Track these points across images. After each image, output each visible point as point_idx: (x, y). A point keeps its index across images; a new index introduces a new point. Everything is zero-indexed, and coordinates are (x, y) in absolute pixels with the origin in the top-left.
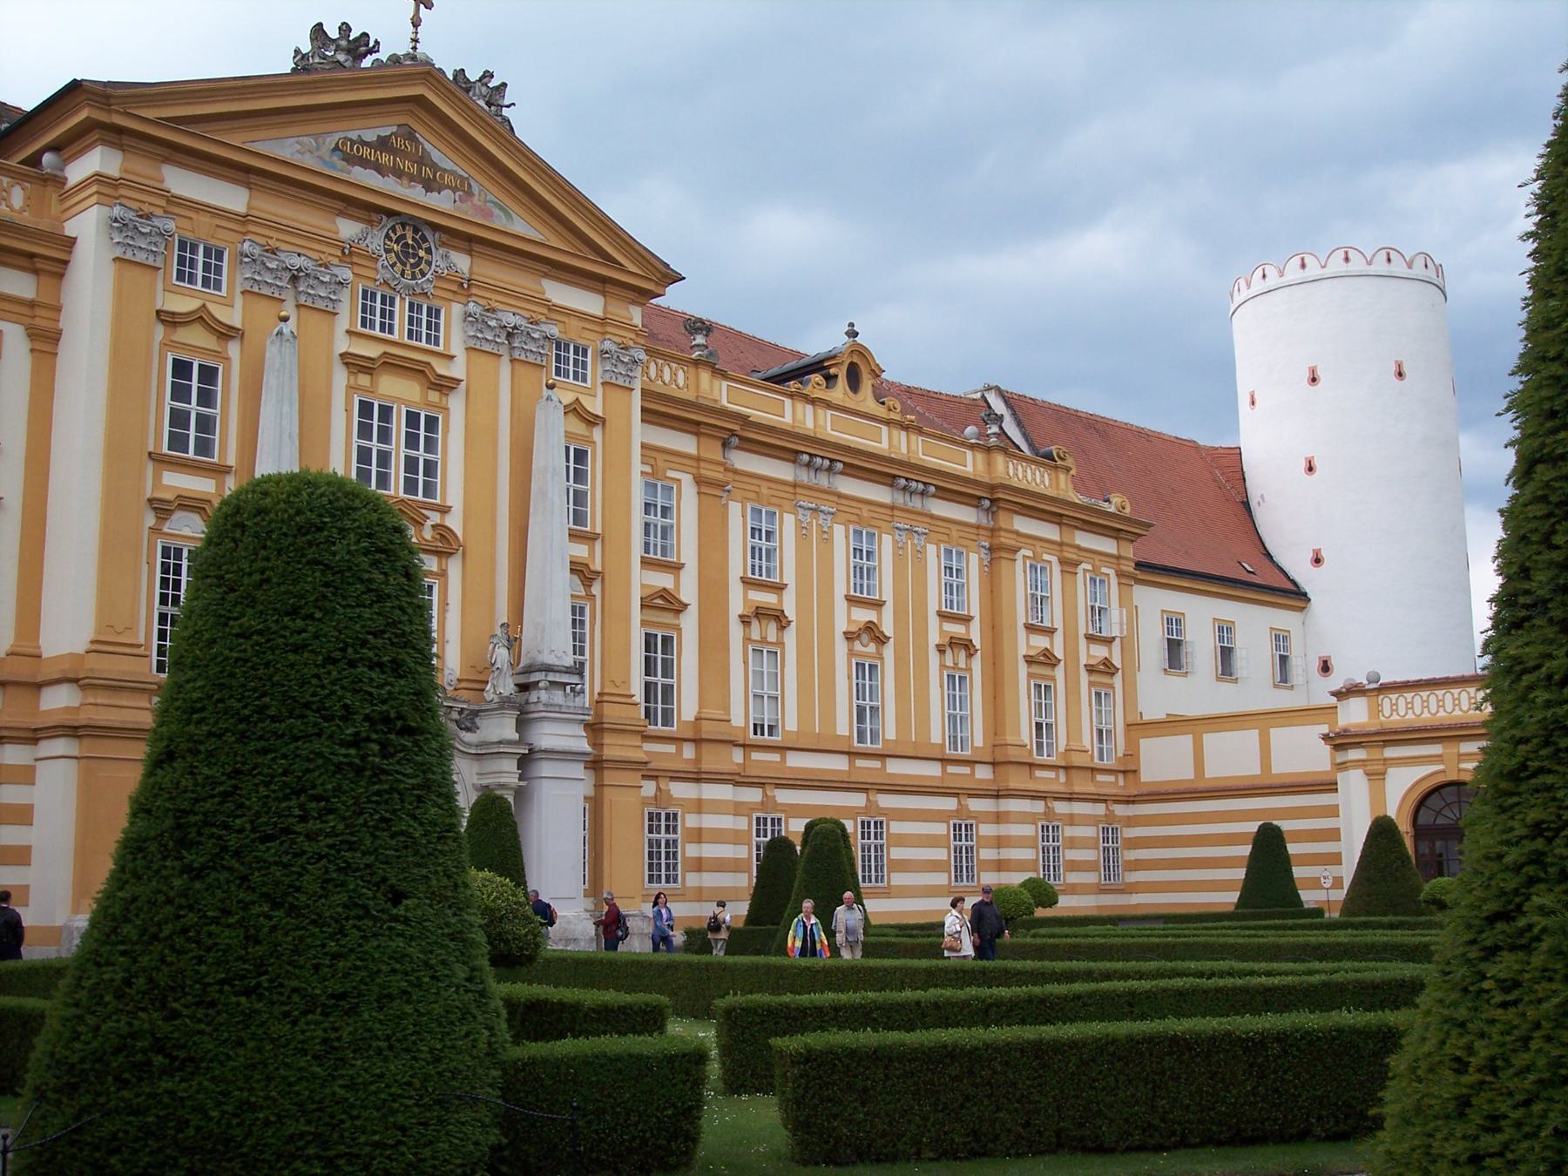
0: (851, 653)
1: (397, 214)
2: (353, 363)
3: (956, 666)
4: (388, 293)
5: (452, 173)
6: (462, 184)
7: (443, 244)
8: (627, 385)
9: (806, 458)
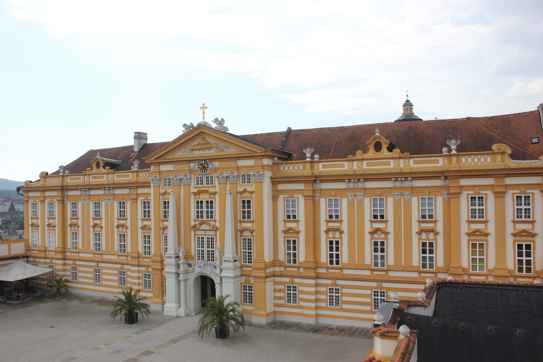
0: (371, 239)
1: (200, 159)
2: (195, 194)
3: (428, 239)
4: (201, 176)
5: (215, 144)
6: (217, 145)
7: (212, 162)
8: (260, 181)
9: (347, 181)
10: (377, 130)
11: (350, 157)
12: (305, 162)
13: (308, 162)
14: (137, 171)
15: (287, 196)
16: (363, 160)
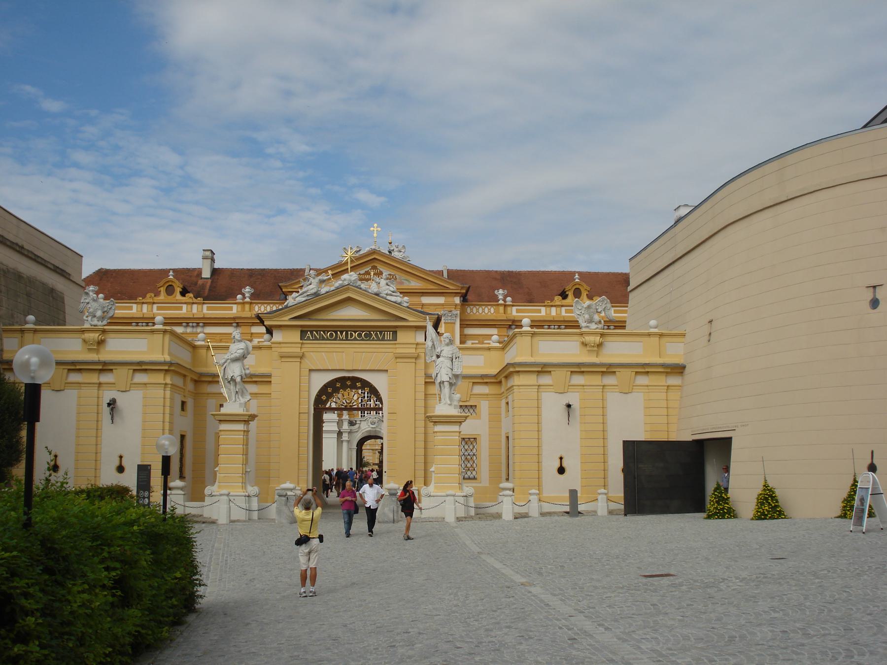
10: (577, 276)
11: (547, 302)
12: (498, 305)
13: (501, 305)
14: (251, 303)
15: (477, 342)
16: (562, 306)
